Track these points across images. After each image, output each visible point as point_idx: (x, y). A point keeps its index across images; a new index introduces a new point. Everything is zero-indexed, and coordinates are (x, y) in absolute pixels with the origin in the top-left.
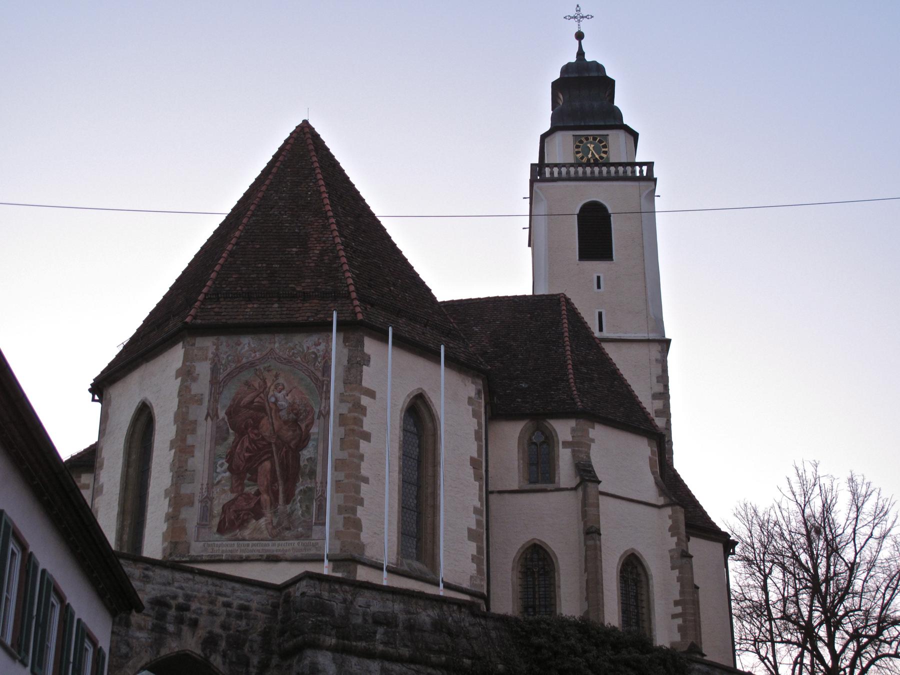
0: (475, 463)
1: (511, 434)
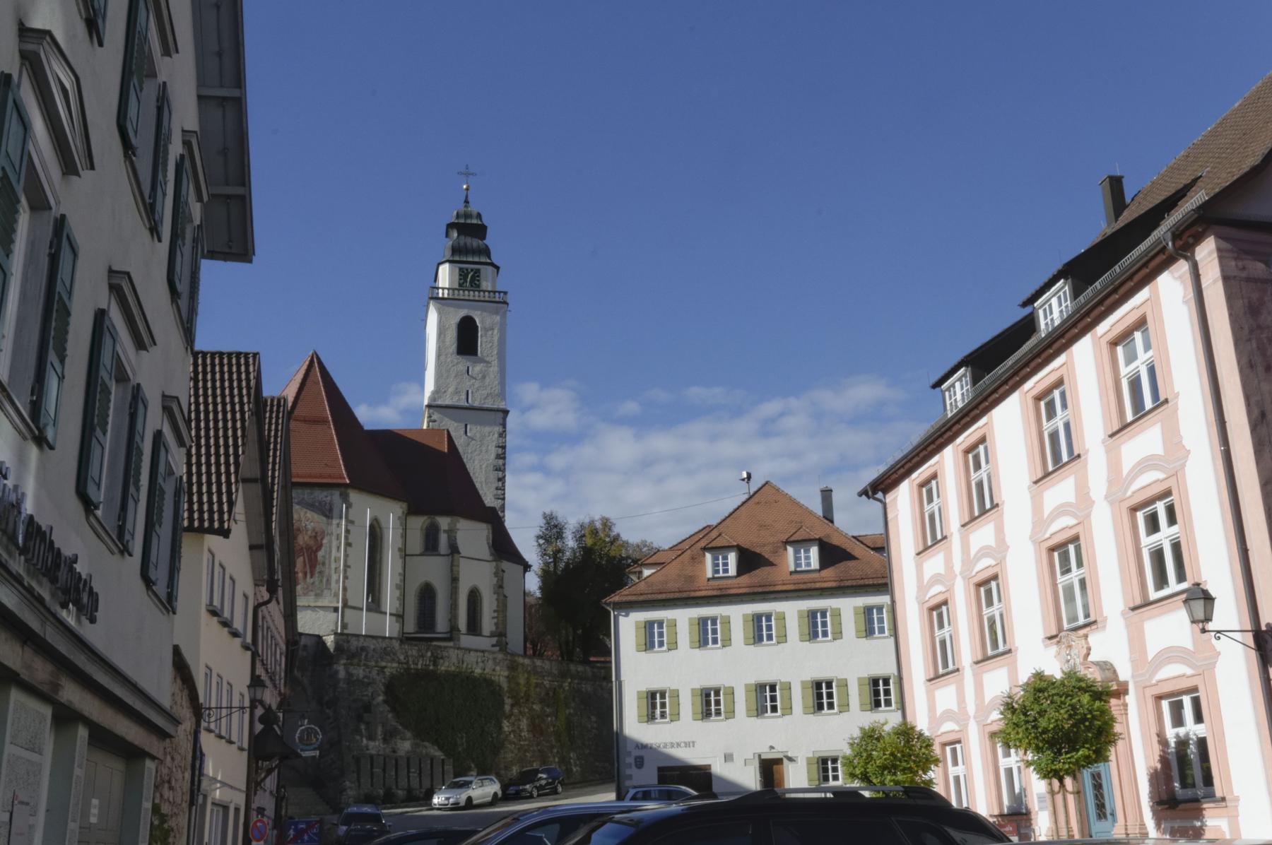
0: (400, 550)
1: (418, 523)
